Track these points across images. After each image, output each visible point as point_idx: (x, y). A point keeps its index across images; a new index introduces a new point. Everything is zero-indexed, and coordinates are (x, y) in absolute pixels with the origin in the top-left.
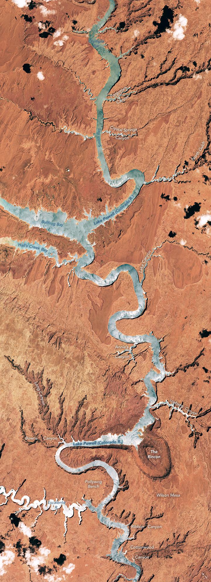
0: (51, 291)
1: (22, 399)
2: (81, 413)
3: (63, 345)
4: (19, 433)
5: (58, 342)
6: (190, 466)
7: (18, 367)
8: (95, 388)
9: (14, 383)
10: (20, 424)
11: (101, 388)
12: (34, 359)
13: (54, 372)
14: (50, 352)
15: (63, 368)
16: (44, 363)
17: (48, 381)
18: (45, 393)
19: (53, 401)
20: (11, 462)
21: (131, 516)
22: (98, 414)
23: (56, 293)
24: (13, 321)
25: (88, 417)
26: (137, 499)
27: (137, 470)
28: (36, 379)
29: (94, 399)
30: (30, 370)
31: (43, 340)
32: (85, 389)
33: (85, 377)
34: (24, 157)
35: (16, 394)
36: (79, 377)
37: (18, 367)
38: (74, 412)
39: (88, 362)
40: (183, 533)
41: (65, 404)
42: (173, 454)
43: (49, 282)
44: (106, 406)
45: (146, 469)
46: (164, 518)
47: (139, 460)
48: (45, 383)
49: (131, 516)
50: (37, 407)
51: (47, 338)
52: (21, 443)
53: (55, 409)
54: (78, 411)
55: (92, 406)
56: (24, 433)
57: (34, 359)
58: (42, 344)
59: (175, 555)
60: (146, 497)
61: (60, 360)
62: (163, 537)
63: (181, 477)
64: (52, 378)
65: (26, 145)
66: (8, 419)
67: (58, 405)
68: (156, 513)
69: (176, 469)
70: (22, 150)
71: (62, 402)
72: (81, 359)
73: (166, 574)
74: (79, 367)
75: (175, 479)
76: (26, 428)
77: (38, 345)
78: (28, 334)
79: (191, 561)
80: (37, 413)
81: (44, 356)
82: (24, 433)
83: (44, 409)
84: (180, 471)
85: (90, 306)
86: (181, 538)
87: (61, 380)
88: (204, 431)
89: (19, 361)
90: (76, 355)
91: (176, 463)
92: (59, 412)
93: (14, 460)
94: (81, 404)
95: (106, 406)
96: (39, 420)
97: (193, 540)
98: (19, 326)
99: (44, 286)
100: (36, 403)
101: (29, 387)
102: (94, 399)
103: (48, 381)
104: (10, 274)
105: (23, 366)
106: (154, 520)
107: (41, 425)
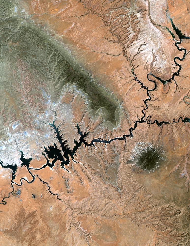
0: (168, 43)
1: (149, 59)
2: (158, 70)
3: (164, 55)
4: (144, 65)
5: (163, 54)
6: (171, 96)
7: (153, 52)
8: (164, 67)
9: (150, 54)
10: (145, 63)
11: (165, 68)
12: (156, 53)
13: (158, 58)
14: (160, 54)
15: (160, 59)
16: (158, 55)
17: (156, 59)
18: (154, 60)
19: (154, 64)
20: (139, 69)
21: (153, 96)
22: (161, 72)
23: (169, 45)
24: (158, 43)
25: (159, 72)
26: (157, 94)
27: (160, 89)
28: (154, 57)
29: (162, 69)
30: (154, 55)
31: (161, 51)
32: (162, 66)
33: (163, 64)
34: (181, 16)
35: (149, 57)
36: (162, 63)
37: (153, 52)
38: (157, 69)
39: (166, 61)
40: (160, 107)
41: (156, 66)
43: (169, 42)
44: (163, 72)
45: (162, 90)
46: (159, 102)
47: (162, 87)
48: (155, 59)
49: (153, 96)
50: (151, 62)
51: (162, 51)
52: (143, 67)
53: (154, 65)
54: (158, 69)
56: (145, 66)
57: (156, 53)
58: (160, 51)
59: (156, 110)
60: (159, 95)
61: (161, 57)
62: (156, 105)
63: (168, 96)
64: (157, 59)
65: (183, 14)
66: (144, 61)
67: (155, 65)
68: (158, 99)
69: (168, 94)
70: (182, 15)
71: (156, 65)
72: (165, 60)
73: (151, 112)
74: (164, 61)
75: (166, 96)
76: (146, 65)
77: (159, 51)
78: (159, 48)
79: (158, 114)
80: (150, 64)
81: (159, 54)
82: (145, 66)
83: (152, 64)
84: (168, 96)
85: (173, 52)
86: (159, 108)
87: (158, 61)
88: (178, 91)
89: (154, 51)
90: (165, 58)
91: (169, 93)
92: (154, 66)
93: (140, 69)
94: (159, 68)
95: (163, 72)
96: (150, 65)
97: (161, 110)
98: (158, 45)
99: (168, 42)
100: (151, 61)
101: (152, 58)
102: (162, 69)
103: (156, 59)
104: (164, 35)
105: (154, 53)
106: (157, 101)
107: (149, 66)
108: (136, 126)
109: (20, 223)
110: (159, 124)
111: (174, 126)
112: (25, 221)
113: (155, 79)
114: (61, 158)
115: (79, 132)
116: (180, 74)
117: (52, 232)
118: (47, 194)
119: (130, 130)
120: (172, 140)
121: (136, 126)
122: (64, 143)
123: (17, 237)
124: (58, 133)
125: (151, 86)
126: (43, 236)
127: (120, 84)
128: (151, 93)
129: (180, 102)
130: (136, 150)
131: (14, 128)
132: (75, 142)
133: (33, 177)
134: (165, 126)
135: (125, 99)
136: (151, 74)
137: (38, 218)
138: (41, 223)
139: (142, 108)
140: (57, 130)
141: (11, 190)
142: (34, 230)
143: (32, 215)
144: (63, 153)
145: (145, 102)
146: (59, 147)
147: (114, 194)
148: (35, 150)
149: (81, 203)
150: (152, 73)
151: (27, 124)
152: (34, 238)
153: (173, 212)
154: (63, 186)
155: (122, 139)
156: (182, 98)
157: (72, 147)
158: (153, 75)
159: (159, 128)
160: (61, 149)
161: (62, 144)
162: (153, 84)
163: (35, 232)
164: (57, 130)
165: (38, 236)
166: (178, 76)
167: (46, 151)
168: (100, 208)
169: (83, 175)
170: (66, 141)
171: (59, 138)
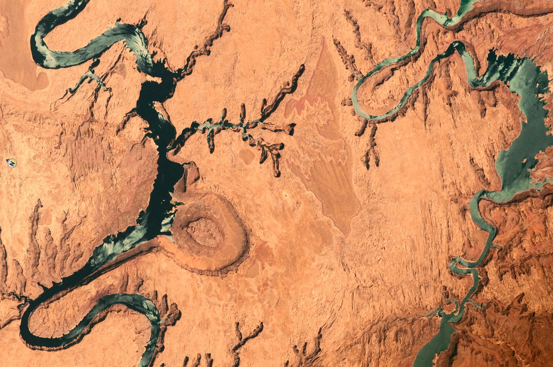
2: (41, 236)
8: (50, 178)
11: (62, 170)
25: (57, 236)
26: (205, 325)
32: (35, 190)
38: (27, 240)
42: (241, 211)
44: (83, 198)
47: (180, 255)
54: (33, 234)
55: (56, 215)
63: (273, 242)
68: (246, 331)
75: (264, 251)
84: (268, 232)
86: (311, 348)
91: (253, 223)
94: (35, 220)
95: (83, 198)
102: (57, 198)
106: (250, 344)
113: (92, 289)
116: (176, 63)
129: (370, 159)
136: (34, 305)
150: (34, 292)
158: (49, 294)
166: (181, 85)
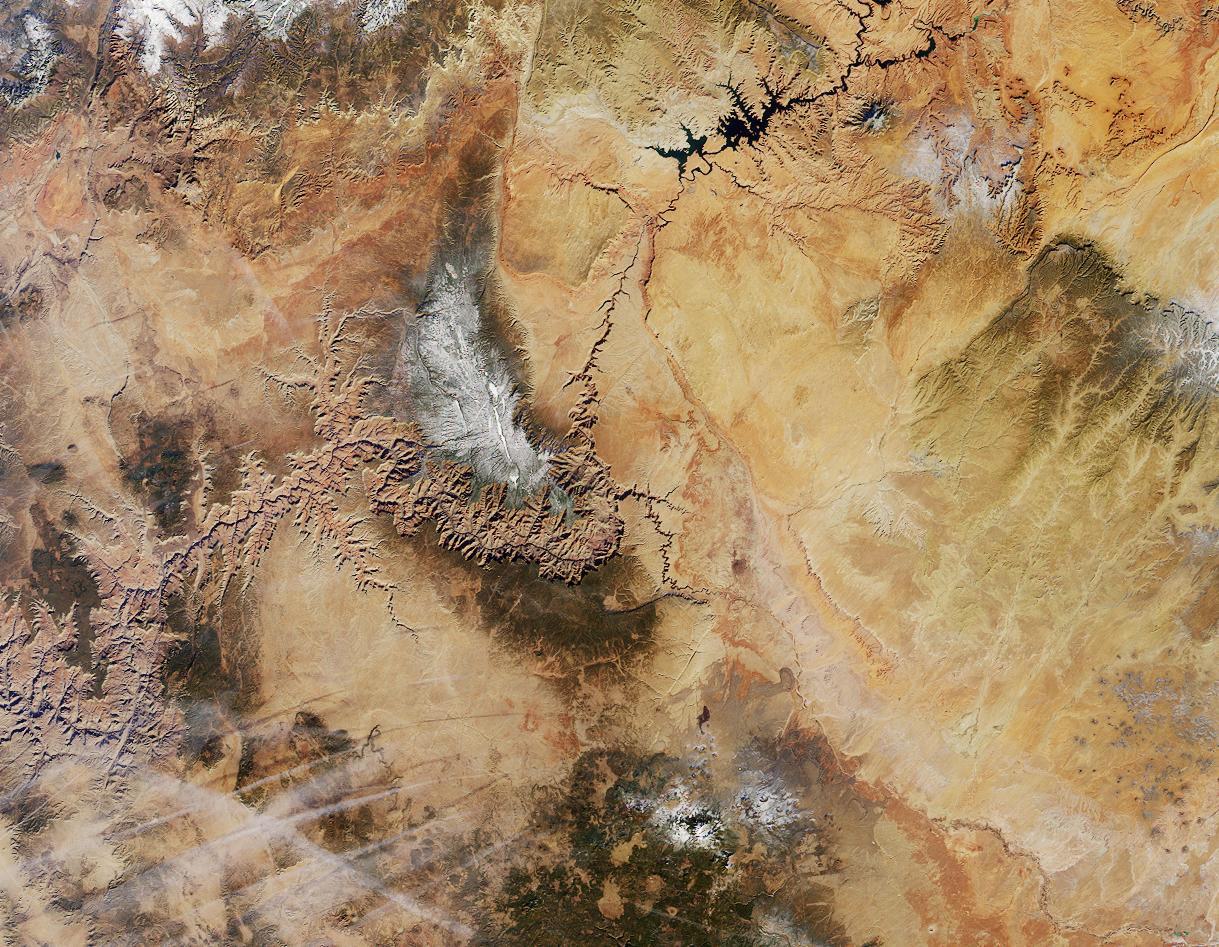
108: (849, 71)
109: (699, 235)
110: (884, 65)
111: (904, 64)
112: (707, 231)
114: (745, 133)
115: (769, 93)
117: (749, 241)
118: (733, 188)
119: (843, 78)
120: (905, 87)
121: (849, 71)
122: (748, 111)
123: (699, 256)
124: (738, 97)
125: (865, 11)
126: (736, 249)
127: (819, 15)
128: (865, 21)
130: (853, 106)
131: (672, 98)
132: (764, 107)
133: (711, 165)
134: (891, 67)
135: (829, 35)
137: (724, 223)
138: (730, 231)
139: (855, 45)
140: (735, 92)
141: (680, 189)
142: (721, 242)
143: (716, 220)
144: (748, 126)
145: (858, 35)
146: (741, 116)
147: (831, 174)
148: (705, 124)
149: (784, 194)
151: (692, 86)
152: (722, 253)
153: (920, 189)
154: (755, 172)
155: (831, 93)
156: (911, 22)
157: (759, 113)
159: (884, 71)
160: (745, 120)
161: (746, 113)
162: (867, 7)
163: (723, 245)
164: (735, 92)
165: (729, 250)
167: (723, 125)
168: (812, 199)
169: (782, 152)
170: (751, 107)
171: (740, 104)
